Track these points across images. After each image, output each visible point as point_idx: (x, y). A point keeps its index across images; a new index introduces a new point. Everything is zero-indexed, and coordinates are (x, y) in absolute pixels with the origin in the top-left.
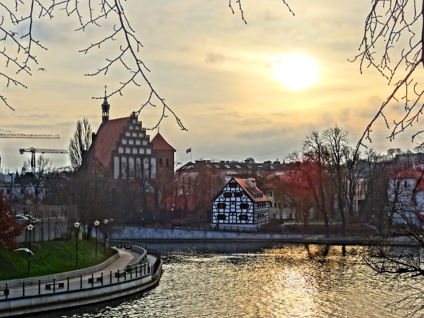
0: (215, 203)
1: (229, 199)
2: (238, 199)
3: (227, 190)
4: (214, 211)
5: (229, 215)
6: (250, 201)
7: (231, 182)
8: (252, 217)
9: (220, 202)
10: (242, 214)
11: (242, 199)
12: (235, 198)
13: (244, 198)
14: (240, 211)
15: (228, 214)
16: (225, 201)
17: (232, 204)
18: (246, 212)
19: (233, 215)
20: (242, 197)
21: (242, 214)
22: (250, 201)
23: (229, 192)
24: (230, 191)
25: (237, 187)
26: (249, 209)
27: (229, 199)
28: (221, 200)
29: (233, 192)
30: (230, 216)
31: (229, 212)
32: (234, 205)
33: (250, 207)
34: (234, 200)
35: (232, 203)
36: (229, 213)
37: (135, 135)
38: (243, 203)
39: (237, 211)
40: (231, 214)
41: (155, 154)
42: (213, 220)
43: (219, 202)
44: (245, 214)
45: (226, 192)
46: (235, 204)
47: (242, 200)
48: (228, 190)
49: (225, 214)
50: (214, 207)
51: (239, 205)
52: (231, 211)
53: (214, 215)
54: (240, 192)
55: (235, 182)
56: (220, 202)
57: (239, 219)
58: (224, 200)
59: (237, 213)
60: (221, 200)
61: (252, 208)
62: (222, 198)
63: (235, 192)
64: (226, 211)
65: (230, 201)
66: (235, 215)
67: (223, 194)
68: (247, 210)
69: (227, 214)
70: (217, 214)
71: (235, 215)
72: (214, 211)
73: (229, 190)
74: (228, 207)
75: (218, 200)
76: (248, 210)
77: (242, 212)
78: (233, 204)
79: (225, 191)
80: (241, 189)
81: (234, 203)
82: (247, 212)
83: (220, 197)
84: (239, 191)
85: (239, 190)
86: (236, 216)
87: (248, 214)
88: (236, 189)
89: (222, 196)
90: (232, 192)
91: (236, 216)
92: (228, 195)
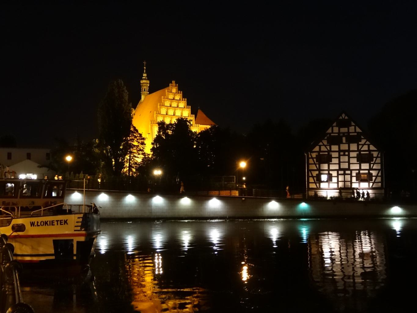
0: (312, 154)
1: (337, 146)
2: (354, 147)
3: (332, 132)
4: (310, 168)
5: (338, 174)
6: (376, 149)
7: (341, 118)
8: (380, 178)
9: (321, 153)
10: (361, 172)
11: (360, 147)
12: (347, 145)
13: (365, 144)
14: (357, 167)
15: (336, 172)
16: (330, 151)
17: (342, 155)
18: (368, 168)
19: (344, 174)
20: (360, 143)
21: (361, 172)
22: (375, 149)
23: (337, 134)
24: (339, 133)
25: (351, 126)
26: (374, 164)
27: (337, 146)
28: (323, 149)
29: (344, 136)
30: (339, 176)
31: (338, 168)
32: (347, 157)
33: (374, 159)
34: (347, 149)
35: (342, 153)
36: (338, 171)
37: (174, 104)
38: (362, 153)
39: (352, 167)
40: (340, 172)
41: (196, 126)
42: (309, 183)
43: (320, 151)
44: (367, 172)
45: (332, 135)
46: (349, 155)
47: (360, 149)
48: (334, 132)
49: (331, 172)
50: (311, 161)
51: (356, 156)
52: (341, 167)
53: (310, 175)
54: (356, 134)
55: (346, 118)
56: (321, 153)
57: (357, 180)
58: (329, 150)
59: (351, 171)
60: (323, 149)
61: (380, 162)
62: (324, 145)
63: (345, 134)
64: (332, 167)
65: (339, 151)
66: (348, 174)
67: (326, 138)
68: (370, 166)
69: (334, 174)
70: (317, 172)
71: (348, 174)
72: (310, 168)
73: (337, 131)
74: (335, 161)
75: (317, 149)
76: (372, 165)
77: (360, 169)
78: (344, 155)
79: (330, 134)
80: (358, 130)
81: (347, 153)
82: (370, 169)
83: (321, 144)
84: (355, 132)
85: (354, 131)
86: (350, 176)
87: (371, 172)
88: (348, 130)
89: (325, 142)
90: (341, 135)
91: (349, 176)
92: (337, 141)
